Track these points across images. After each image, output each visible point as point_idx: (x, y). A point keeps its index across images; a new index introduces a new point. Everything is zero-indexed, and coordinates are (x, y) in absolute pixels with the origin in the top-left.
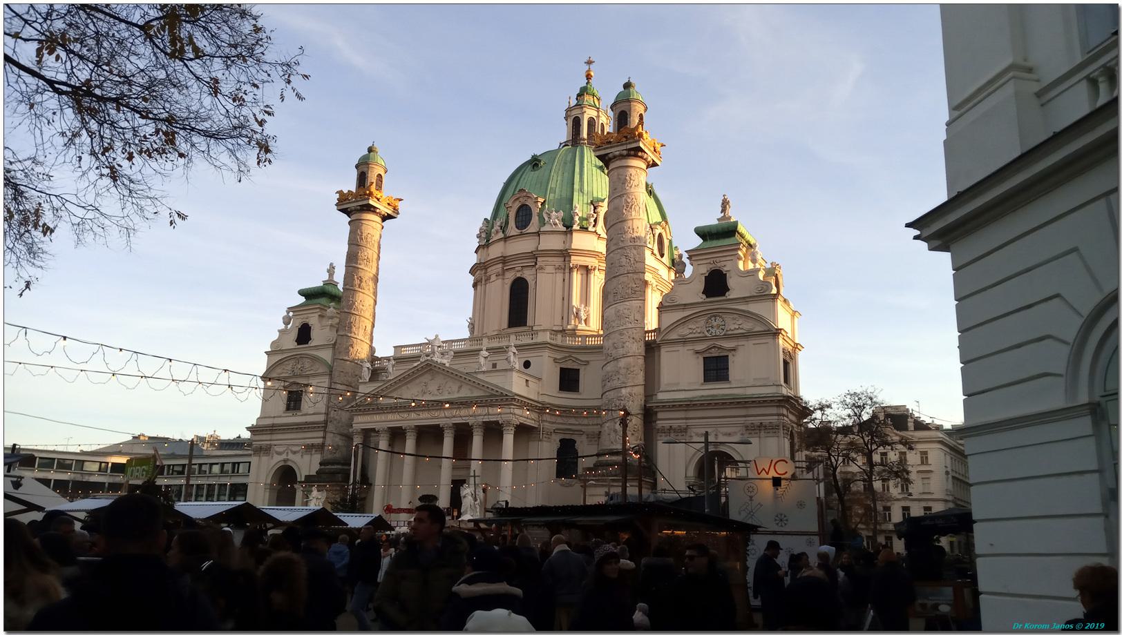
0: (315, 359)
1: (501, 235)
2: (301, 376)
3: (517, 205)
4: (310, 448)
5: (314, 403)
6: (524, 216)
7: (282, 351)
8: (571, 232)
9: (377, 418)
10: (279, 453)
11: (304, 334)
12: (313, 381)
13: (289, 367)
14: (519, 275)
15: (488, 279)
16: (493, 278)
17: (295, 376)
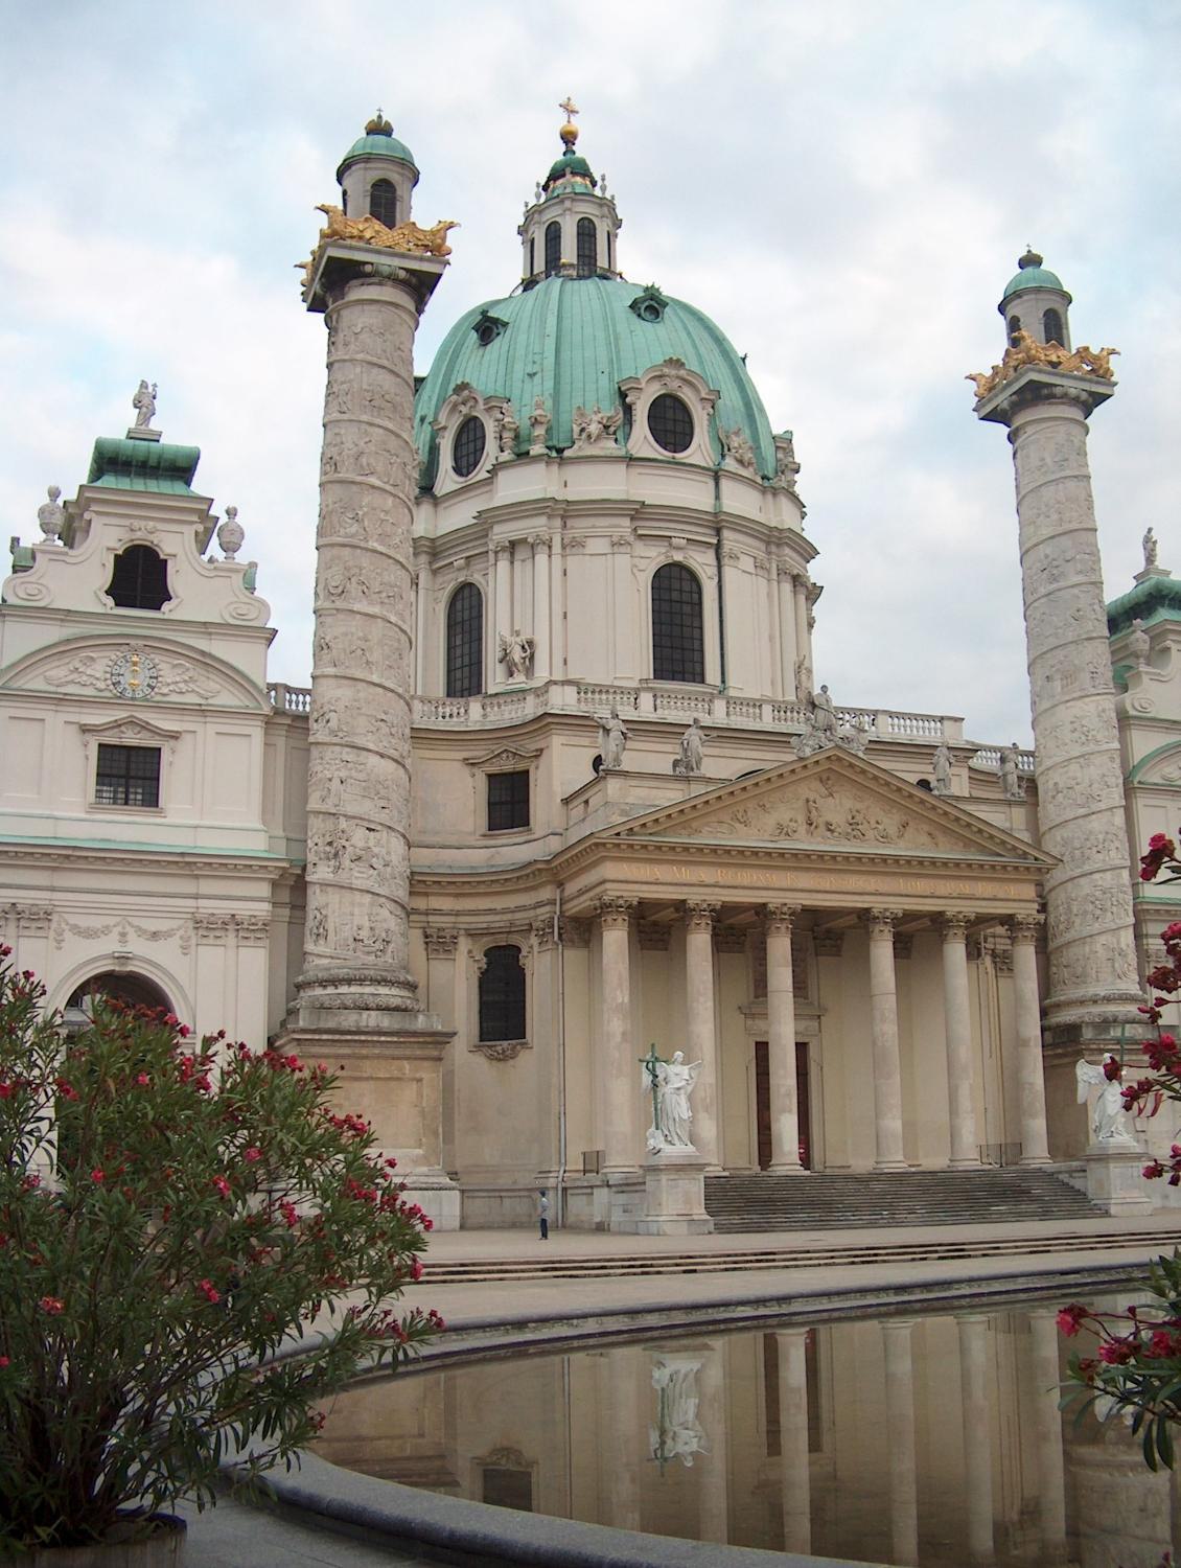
0: (207, 662)
1: (609, 446)
2: (160, 707)
3: (653, 391)
4: (207, 927)
5: (217, 796)
6: (672, 423)
7: (67, 616)
8: (775, 492)
9: (686, 874)
10: (89, 934)
11: (140, 578)
12: (208, 730)
13: (99, 669)
14: (678, 557)
15: (572, 545)
16: (597, 545)
17: (120, 699)
